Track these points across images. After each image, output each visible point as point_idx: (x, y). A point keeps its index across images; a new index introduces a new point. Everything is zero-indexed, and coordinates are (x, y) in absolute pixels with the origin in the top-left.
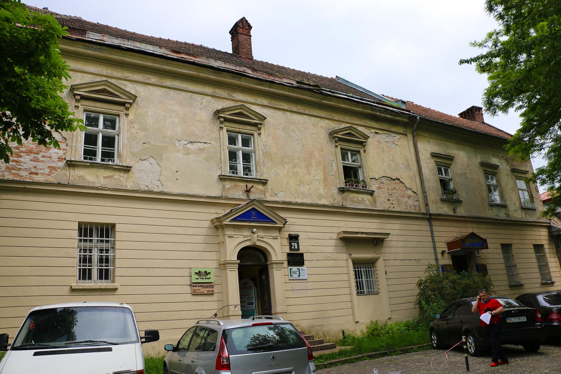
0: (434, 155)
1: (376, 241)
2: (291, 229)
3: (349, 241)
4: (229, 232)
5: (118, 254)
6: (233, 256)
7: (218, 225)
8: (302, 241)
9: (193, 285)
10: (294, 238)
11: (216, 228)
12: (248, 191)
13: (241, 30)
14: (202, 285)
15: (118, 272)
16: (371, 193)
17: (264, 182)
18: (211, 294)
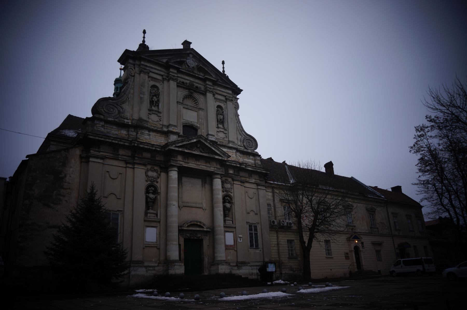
0: (392, 213)
1: (380, 244)
2: (362, 240)
3: (374, 244)
4: (351, 242)
5: (332, 248)
6: (353, 249)
7: (348, 240)
8: (364, 244)
9: (345, 257)
10: (362, 243)
11: (348, 240)
12: (352, 229)
13: (329, 166)
14: (347, 257)
15: (332, 253)
16: (378, 228)
17: (355, 226)
18: (349, 259)
